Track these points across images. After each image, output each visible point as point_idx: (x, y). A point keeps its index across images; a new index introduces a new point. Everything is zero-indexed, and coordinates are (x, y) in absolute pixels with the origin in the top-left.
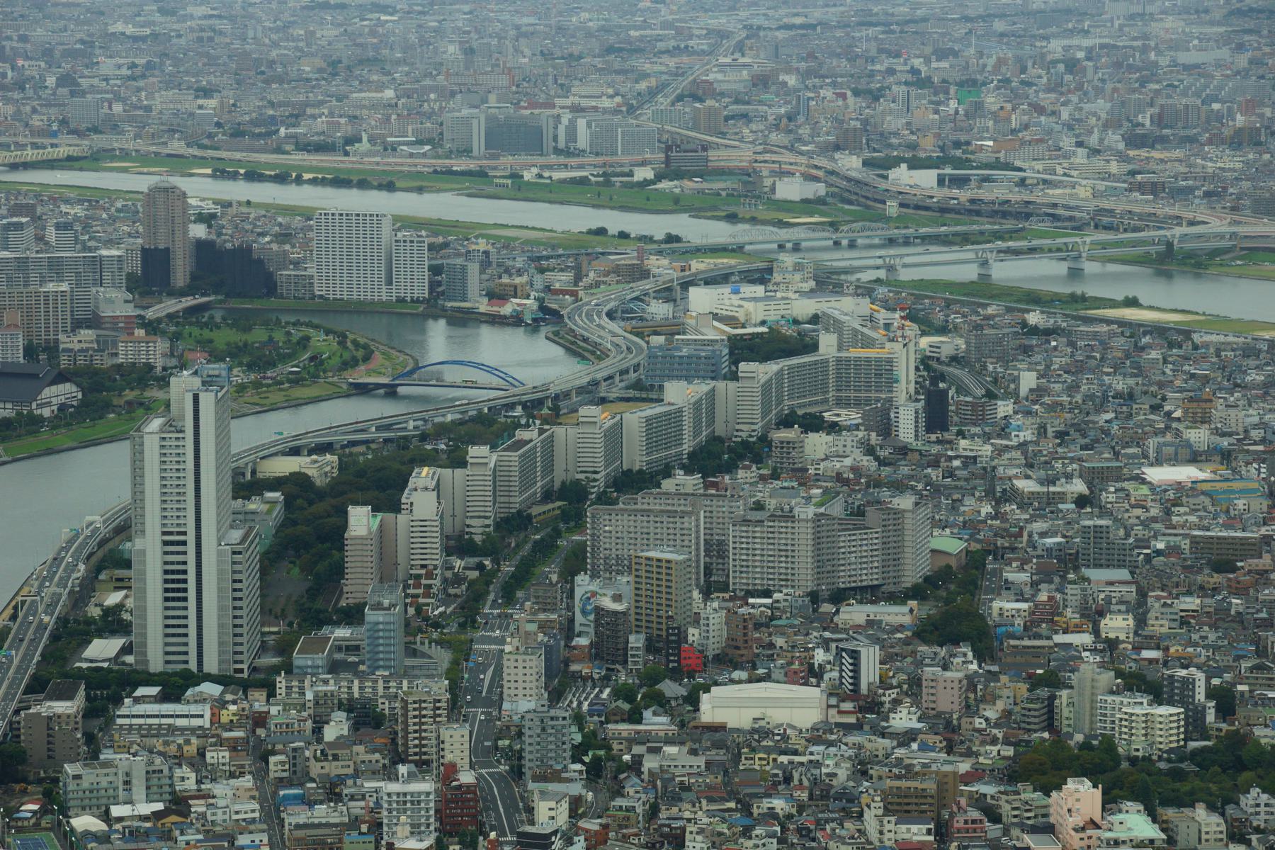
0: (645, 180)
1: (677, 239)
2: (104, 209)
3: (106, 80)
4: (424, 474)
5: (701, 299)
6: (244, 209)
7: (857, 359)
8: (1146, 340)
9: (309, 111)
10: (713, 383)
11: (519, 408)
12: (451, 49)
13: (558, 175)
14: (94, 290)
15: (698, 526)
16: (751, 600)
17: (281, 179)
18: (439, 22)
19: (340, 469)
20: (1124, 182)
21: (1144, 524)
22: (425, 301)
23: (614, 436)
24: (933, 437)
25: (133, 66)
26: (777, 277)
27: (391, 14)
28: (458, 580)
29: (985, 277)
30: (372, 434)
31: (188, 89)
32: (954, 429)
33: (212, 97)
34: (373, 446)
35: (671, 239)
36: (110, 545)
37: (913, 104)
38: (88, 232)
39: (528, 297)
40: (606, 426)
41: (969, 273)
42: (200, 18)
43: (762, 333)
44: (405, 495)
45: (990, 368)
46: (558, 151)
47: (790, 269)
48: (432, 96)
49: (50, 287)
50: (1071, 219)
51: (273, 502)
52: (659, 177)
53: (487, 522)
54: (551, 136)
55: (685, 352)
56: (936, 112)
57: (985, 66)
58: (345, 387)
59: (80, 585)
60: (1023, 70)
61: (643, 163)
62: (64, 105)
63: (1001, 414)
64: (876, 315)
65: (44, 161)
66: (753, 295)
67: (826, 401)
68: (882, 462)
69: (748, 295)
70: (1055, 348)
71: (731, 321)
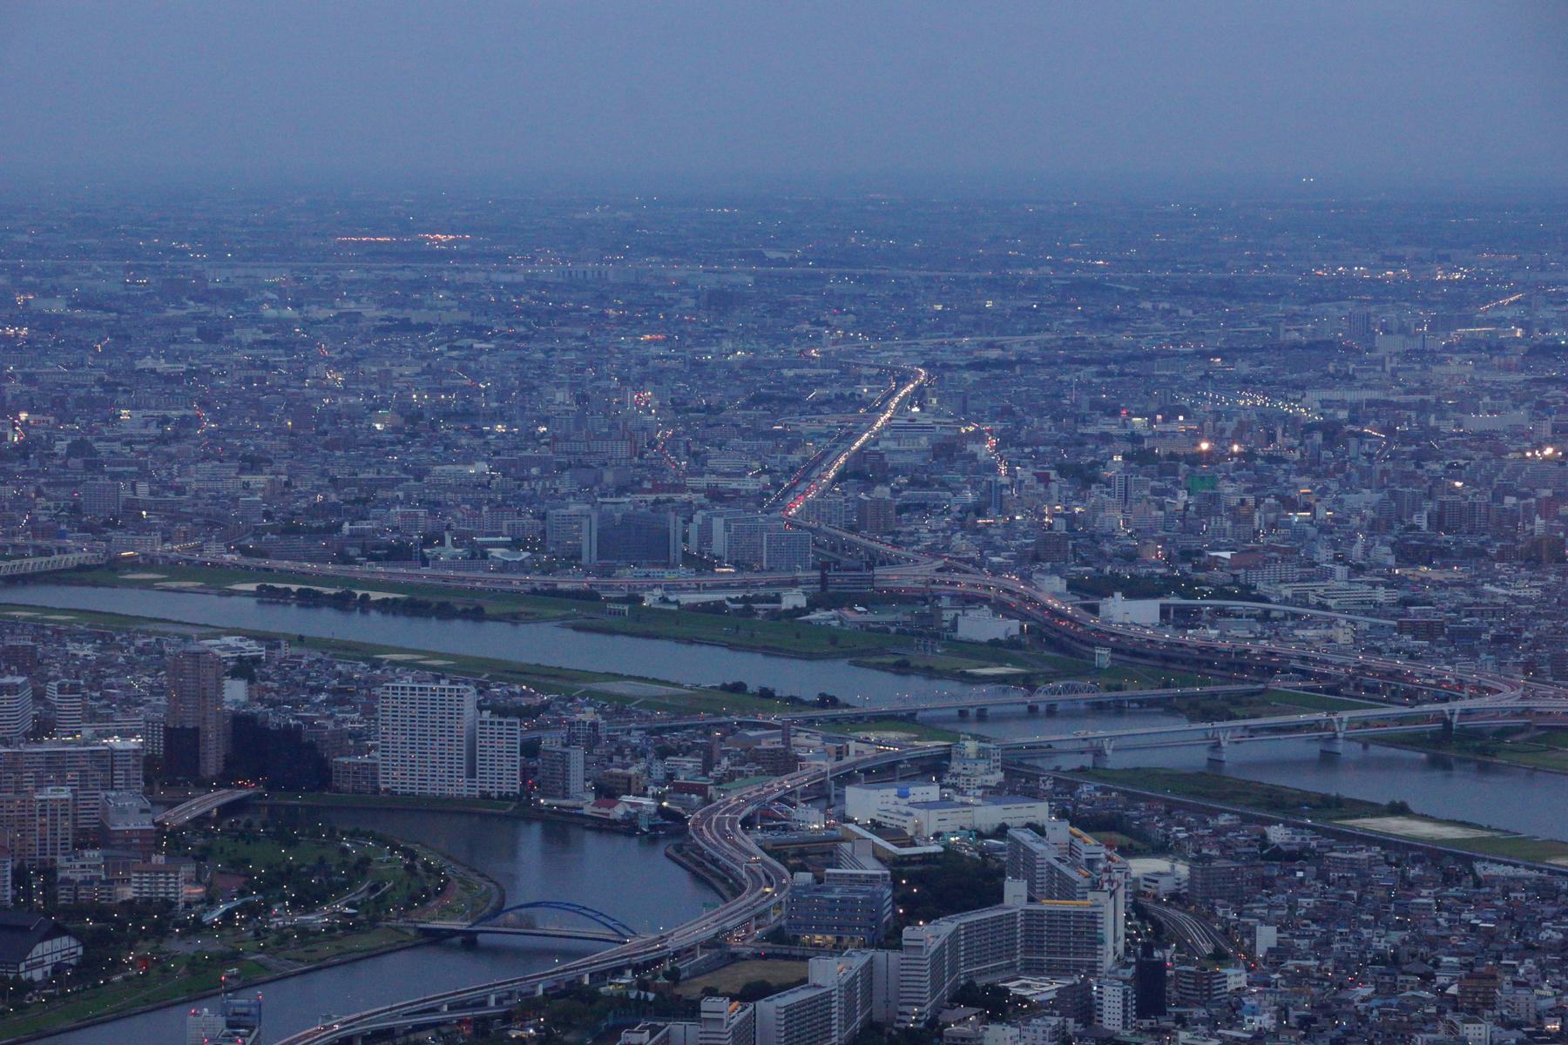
0: (795, 608)
1: (835, 702)
2: (121, 649)
3: (129, 443)
5: (864, 803)
6: (295, 650)
7: (1050, 914)
8: (1414, 872)
9: (381, 494)
10: (871, 952)
11: (629, 973)
12: (560, 396)
13: (687, 598)
14: (103, 795)
17: (343, 603)
18: (546, 352)
20: (1393, 617)
22: (517, 797)
24: (1146, 1023)
25: (165, 420)
26: (956, 766)
27: (487, 340)
29: (1215, 763)
30: (445, 1014)
31: (232, 456)
32: (1173, 1010)
33: (261, 472)
34: (445, 1030)
35: (826, 701)
37: (1134, 494)
38: (99, 688)
39: (645, 795)
40: (735, 1022)
41: (1197, 757)
42: (250, 346)
43: (935, 854)
45: (1220, 912)
46: (688, 559)
47: (973, 756)
48: (534, 471)
49: (48, 793)
50: (1326, 677)
52: (813, 605)
54: (679, 537)
55: (837, 894)
56: (1161, 507)
57: (1223, 430)
58: (412, 932)
60: (1272, 438)
61: (794, 583)
62: (76, 484)
63: (1231, 987)
64: (1077, 842)
65: (48, 573)
66: (925, 798)
67: (1012, 966)
69: (918, 799)
70: (1302, 880)
71: (897, 836)
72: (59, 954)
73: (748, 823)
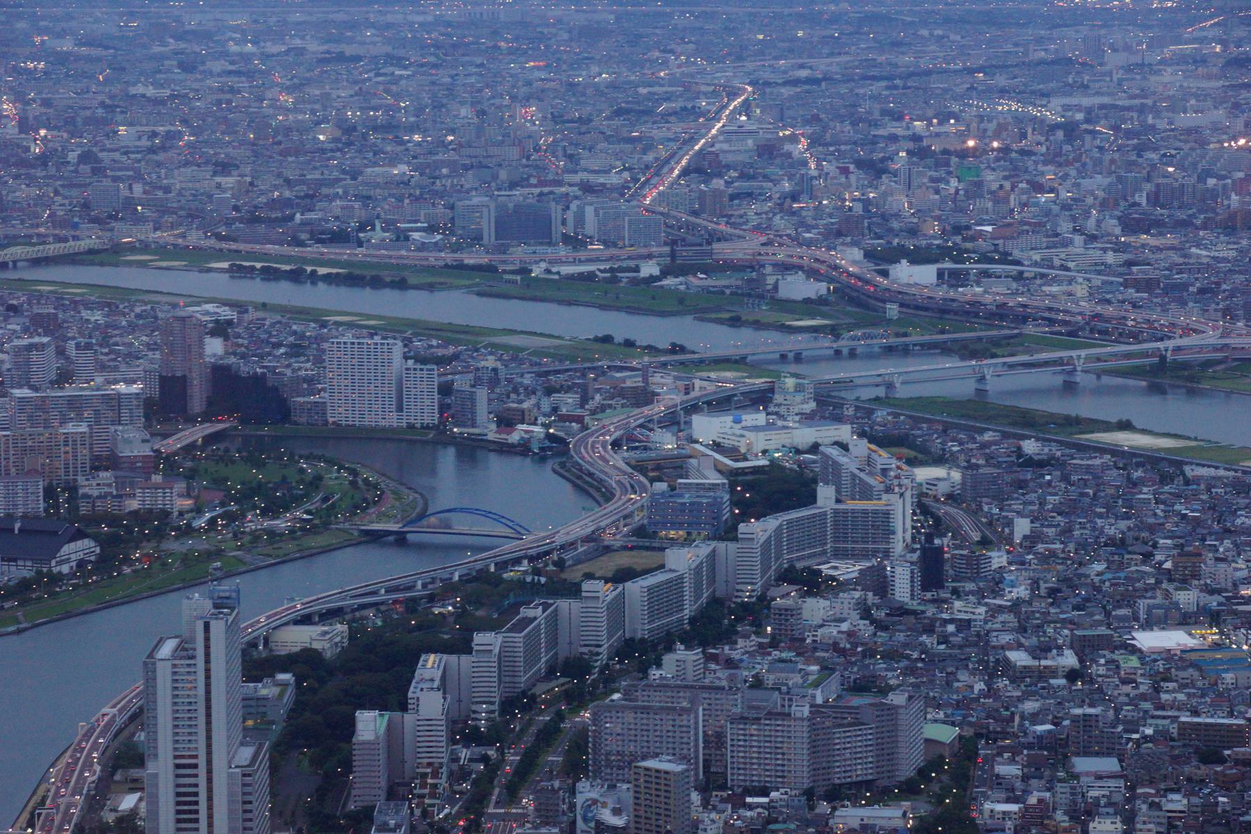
0: (651, 276)
1: (683, 349)
2: (124, 315)
3: (126, 153)
4: (429, 664)
5: (707, 427)
6: (260, 314)
7: (853, 511)
8: (1138, 474)
9: (325, 191)
10: (714, 544)
11: (525, 562)
12: (464, 112)
13: (566, 270)
14: (112, 428)
15: (696, 723)
16: (749, 800)
17: (296, 276)
18: (452, 77)
19: (350, 639)
20: (1120, 275)
21: (1133, 702)
22: (435, 427)
23: (617, 608)
24: (929, 595)
25: (154, 135)
26: (778, 398)
27: (405, 68)
28: (463, 774)
29: (981, 392)
30: (382, 596)
31: (206, 163)
32: (950, 585)
33: (229, 174)
34: (383, 608)
35: (676, 349)
36: (126, 733)
37: (915, 183)
38: (108, 346)
39: (535, 424)
40: (609, 599)
41: (964, 389)
42: (219, 75)
43: (763, 466)
44: (412, 689)
45: (986, 508)
46: (566, 239)
47: (792, 390)
48: (445, 171)
49: (70, 428)
50: (1065, 323)
51: (285, 685)
52: (665, 273)
53: (492, 707)
54: (559, 221)
55: (686, 499)
56: (937, 192)
57: (985, 130)
58: (356, 533)
59: (96, 788)
60: (1023, 136)
61: (650, 256)
62: (85, 186)
64: (874, 456)
65: (65, 255)
66: (754, 423)
67: (824, 552)
68: (880, 626)
70: (1049, 482)
71: (733, 453)
72: (81, 553)
73: (616, 444)
